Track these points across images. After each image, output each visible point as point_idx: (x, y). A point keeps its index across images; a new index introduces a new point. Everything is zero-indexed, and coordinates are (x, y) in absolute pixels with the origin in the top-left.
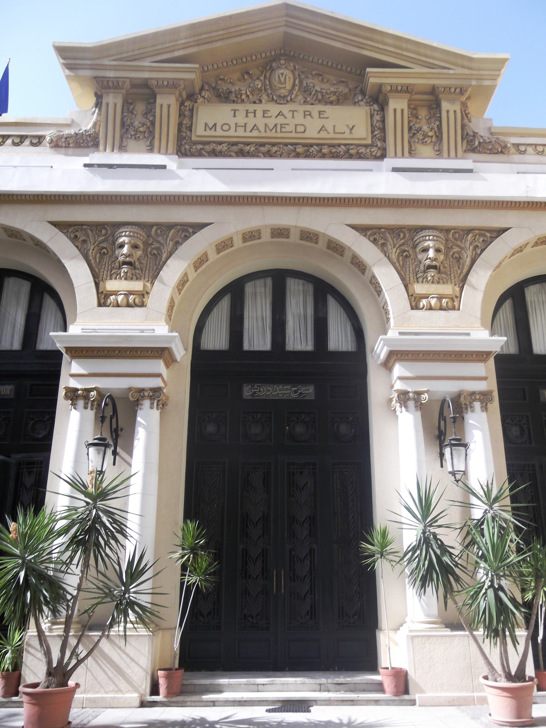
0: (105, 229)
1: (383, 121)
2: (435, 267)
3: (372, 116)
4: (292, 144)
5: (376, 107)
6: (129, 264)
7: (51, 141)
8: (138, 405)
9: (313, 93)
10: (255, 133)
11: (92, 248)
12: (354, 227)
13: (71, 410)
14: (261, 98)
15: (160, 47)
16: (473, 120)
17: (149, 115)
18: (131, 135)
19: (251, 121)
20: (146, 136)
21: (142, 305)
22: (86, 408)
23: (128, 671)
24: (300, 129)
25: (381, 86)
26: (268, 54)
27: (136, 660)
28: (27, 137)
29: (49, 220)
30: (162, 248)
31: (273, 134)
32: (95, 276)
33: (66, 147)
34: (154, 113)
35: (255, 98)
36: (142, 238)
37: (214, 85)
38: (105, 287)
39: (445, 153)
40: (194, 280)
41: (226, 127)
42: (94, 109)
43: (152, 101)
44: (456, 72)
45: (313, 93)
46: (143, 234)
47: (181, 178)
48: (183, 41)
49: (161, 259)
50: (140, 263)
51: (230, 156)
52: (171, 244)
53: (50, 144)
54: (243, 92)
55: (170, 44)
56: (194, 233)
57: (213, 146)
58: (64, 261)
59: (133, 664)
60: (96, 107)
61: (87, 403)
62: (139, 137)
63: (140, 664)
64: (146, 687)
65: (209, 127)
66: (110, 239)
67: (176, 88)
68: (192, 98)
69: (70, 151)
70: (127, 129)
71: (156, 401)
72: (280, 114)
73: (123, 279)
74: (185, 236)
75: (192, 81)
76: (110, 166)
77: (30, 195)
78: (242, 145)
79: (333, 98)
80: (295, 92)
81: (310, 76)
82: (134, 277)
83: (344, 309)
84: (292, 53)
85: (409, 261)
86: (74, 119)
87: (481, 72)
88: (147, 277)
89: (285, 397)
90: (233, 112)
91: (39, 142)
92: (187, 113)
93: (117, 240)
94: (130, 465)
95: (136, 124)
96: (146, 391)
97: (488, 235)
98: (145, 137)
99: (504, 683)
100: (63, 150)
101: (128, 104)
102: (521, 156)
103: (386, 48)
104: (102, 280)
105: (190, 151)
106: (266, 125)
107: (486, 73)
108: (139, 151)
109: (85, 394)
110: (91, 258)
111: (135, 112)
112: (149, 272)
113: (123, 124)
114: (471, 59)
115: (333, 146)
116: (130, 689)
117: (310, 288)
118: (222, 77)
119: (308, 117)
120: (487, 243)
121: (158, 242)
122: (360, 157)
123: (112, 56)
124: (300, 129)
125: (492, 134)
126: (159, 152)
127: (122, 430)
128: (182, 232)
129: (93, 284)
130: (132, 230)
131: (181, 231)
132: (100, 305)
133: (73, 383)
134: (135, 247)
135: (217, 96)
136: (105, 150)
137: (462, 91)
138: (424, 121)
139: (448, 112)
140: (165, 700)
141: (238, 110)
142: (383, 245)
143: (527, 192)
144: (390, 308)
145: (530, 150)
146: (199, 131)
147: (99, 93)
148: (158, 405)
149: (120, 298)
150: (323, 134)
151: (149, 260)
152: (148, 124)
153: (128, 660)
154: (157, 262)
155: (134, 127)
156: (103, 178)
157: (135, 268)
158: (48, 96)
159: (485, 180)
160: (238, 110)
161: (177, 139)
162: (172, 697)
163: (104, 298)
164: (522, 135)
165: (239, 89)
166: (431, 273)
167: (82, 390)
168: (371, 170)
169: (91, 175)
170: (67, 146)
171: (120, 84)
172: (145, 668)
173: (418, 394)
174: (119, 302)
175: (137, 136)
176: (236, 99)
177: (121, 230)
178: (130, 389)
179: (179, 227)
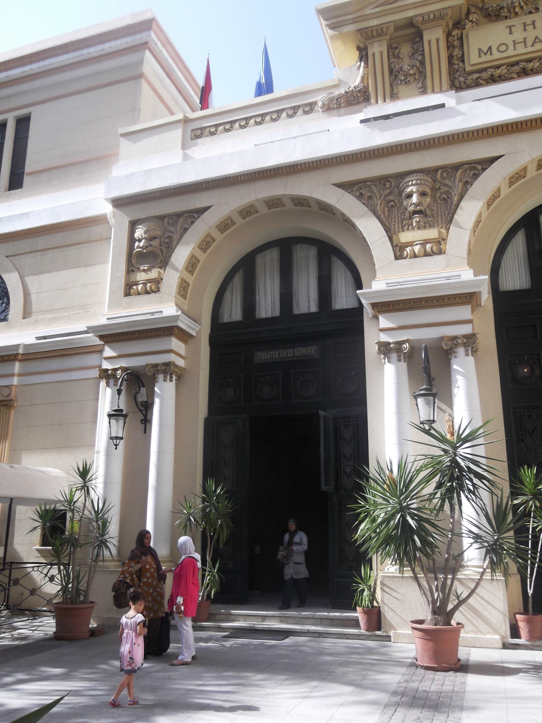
0: (389, 181)
6: (420, 212)
7: (324, 105)
8: (451, 353)
11: (379, 202)
13: (385, 363)
14: (537, 6)
17: (416, 55)
18: (401, 80)
20: (416, 78)
21: (441, 252)
22: (399, 360)
23: (485, 613)
27: (491, 603)
29: (334, 183)
30: (451, 190)
32: (387, 230)
33: (337, 108)
34: (422, 52)
35: (530, 8)
36: (429, 184)
37: (481, 5)
38: (399, 239)
40: (486, 220)
41: (503, 48)
42: (359, 63)
43: (417, 40)
46: (430, 180)
47: (464, 114)
49: (452, 203)
50: (431, 210)
52: (460, 185)
53: (322, 108)
54: (516, 4)
56: (484, 170)
57: (490, 72)
58: (354, 220)
59: (489, 607)
60: (361, 61)
61: (400, 356)
62: (409, 81)
63: (496, 607)
64: (506, 629)
65: (483, 52)
66: (396, 191)
67: (444, 19)
68: (459, 26)
69: (342, 111)
70: (396, 76)
71: (470, 348)
73: (416, 228)
74: (474, 174)
76: (387, 117)
77: (313, 162)
78: (524, 63)
82: (427, 225)
88: (440, 223)
90: (508, 29)
91: (311, 109)
92: (456, 43)
93: (403, 191)
95: (406, 67)
96: (460, 338)
98: (415, 79)
100: (335, 112)
101: (393, 50)
104: (395, 233)
105: (465, 83)
108: (412, 96)
109: (397, 347)
110: (380, 213)
111: (401, 56)
112: (441, 218)
113: (391, 71)
116: (490, 630)
121: (446, 185)
123: (373, 3)
126: (433, 92)
127: (434, 379)
128: (470, 170)
129: (387, 238)
130: (418, 178)
131: (468, 170)
132: (397, 258)
133: (384, 338)
134: (423, 194)
135: (485, 17)
136: (377, 102)
140: (528, 643)
141: (514, 26)
146: (474, 58)
147: (362, 45)
148: (472, 351)
149: (417, 249)
151: (439, 205)
152: (418, 64)
153: (483, 602)
154: (449, 206)
155: (404, 71)
157: (426, 216)
160: (514, 26)
161: (449, 74)
162: (535, 641)
163: (399, 251)
165: (512, 2)
167: (394, 343)
169: (368, 130)
171: (384, 30)
172: (502, 611)
174: (416, 252)
175: (407, 80)
176: (508, 14)
177: (406, 180)
178: (442, 338)
179: (466, 166)
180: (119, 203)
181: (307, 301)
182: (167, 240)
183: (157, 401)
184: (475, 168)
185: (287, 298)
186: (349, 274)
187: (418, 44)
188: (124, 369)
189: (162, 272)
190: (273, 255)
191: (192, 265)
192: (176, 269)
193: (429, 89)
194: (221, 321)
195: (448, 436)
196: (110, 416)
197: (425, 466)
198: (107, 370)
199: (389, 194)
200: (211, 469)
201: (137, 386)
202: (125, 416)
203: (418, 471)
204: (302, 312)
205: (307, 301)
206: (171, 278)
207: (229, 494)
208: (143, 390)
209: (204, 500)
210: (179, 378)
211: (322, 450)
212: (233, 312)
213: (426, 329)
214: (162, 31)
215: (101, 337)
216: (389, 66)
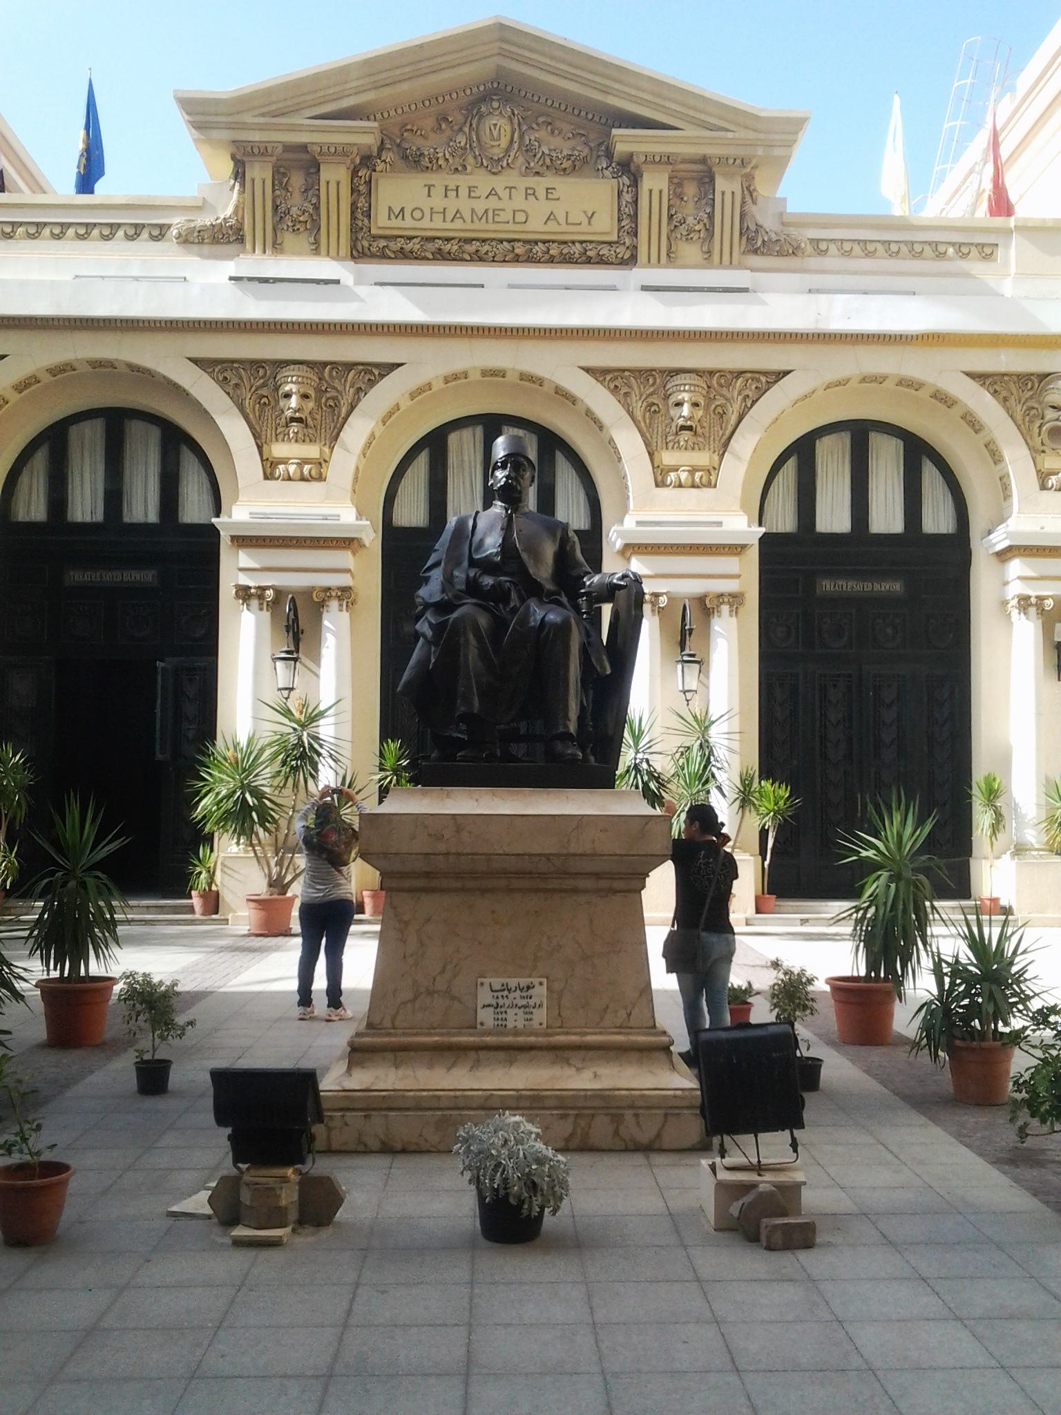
1: (636, 202)
2: (690, 428)
3: (620, 193)
4: (509, 241)
6: (300, 420)
7: (179, 236)
9: (538, 156)
10: (458, 224)
12: (587, 370)
15: (322, 93)
16: (760, 201)
17: (311, 193)
19: (452, 204)
21: (321, 478)
22: (261, 609)
24: (520, 217)
25: (632, 155)
26: (475, 90)
28: (143, 226)
31: (482, 225)
32: (256, 436)
35: (455, 162)
39: (716, 258)
41: (417, 214)
43: (312, 170)
44: (737, 135)
45: (538, 156)
48: (355, 84)
50: (314, 419)
55: (338, 89)
56: (382, 376)
57: (400, 243)
69: (206, 249)
72: (493, 192)
76: (265, 280)
79: (566, 164)
80: (512, 154)
81: (534, 126)
83: (577, 472)
84: (509, 89)
85: (659, 419)
86: (208, 199)
94: (317, 676)
95: (294, 211)
97: (763, 379)
100: (195, 247)
101: (280, 176)
102: (820, 259)
106: (473, 210)
107: (777, 137)
113: (276, 208)
114: (757, 118)
115: (565, 243)
118: (409, 127)
119: (531, 198)
120: (761, 392)
122: (602, 262)
124: (520, 217)
125: (783, 224)
126: (328, 254)
132: (266, 478)
133: (244, 580)
134: (305, 396)
137: (743, 164)
138: (691, 205)
139: (723, 193)
143: (817, 321)
144: (629, 483)
145: (833, 248)
146: (381, 221)
147: (238, 157)
149: (292, 469)
150: (552, 227)
158: (170, 167)
159: (764, 303)
164: (825, 226)
166: (686, 435)
170: (202, 242)
171: (270, 150)
184: (371, 373)
185: (114, 497)
187: (314, 176)
195: (297, 714)
197: (270, 744)
199: (264, 385)
203: (262, 750)
204: (135, 521)
205: (143, 506)
211: (158, 711)
213: (298, 573)
216: (274, 201)
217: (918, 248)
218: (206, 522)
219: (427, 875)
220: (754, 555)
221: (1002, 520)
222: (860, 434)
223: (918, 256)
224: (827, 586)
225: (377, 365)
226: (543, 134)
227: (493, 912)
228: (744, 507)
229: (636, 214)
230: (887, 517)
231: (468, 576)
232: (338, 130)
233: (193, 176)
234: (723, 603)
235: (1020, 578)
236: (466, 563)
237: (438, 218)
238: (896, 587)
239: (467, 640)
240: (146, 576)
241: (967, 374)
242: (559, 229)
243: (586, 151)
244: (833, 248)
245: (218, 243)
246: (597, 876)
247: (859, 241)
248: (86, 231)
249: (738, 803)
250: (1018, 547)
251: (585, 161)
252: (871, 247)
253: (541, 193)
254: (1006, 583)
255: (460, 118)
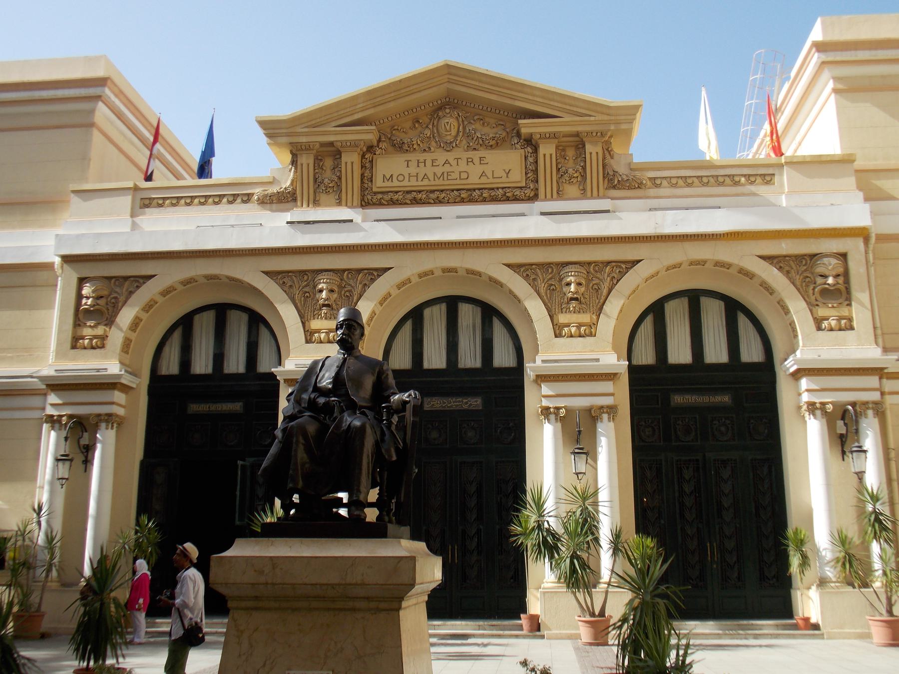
1: (536, 162)
2: (576, 299)
3: (526, 158)
4: (458, 190)
5: (529, 149)
6: (328, 306)
7: (259, 199)
10: (426, 182)
12: (508, 266)
16: (615, 157)
19: (422, 171)
24: (464, 176)
25: (531, 134)
31: (441, 182)
32: (301, 316)
41: (401, 178)
47: (365, 231)
48: (361, 105)
51: (406, 204)
56: (379, 276)
57: (390, 195)
69: (274, 206)
72: (447, 162)
75: (371, 140)
80: (459, 139)
84: (456, 101)
87: (618, 118)
89: (458, 408)
92: (368, 165)
97: (624, 266)
99: (588, 618)
101: (318, 159)
103: (535, 99)
107: (623, 117)
113: (315, 180)
115: (493, 189)
117: (479, 309)
120: (623, 274)
122: (516, 199)
124: (464, 176)
125: (631, 169)
129: (301, 324)
132: (308, 342)
134: (332, 291)
138: (571, 161)
139: (591, 153)
142: (534, 279)
145: (665, 183)
146: (379, 183)
149: (322, 336)
150: (484, 180)
156: (303, 233)
159: (620, 219)
164: (659, 169)
166: (574, 304)
168: (523, 215)
170: (272, 203)
173: (558, 409)
180: (68, 259)
181: (235, 363)
182: (113, 301)
183: (99, 446)
185: (219, 359)
186: (273, 342)
188: (71, 417)
189: (108, 329)
190: (210, 316)
191: (135, 324)
192: (121, 330)
193: (344, 202)
194: (159, 373)
196: (58, 460)
198: (52, 416)
199: (306, 286)
200: (144, 506)
201: (80, 434)
202: (71, 460)
205: (235, 363)
206: (116, 337)
207: (159, 526)
208: (86, 435)
209: (136, 532)
210: (119, 424)
211: (238, 493)
212: (171, 366)
214: (115, 85)
215: (48, 385)
216: (314, 176)
217: (721, 179)
218: (268, 371)
219: (256, 598)
220: (625, 379)
221: (794, 351)
222: (694, 299)
223: (722, 184)
224: (678, 399)
225: (376, 270)
226: (478, 126)
227: (299, 625)
228: (616, 348)
229: (537, 169)
230: (716, 352)
231: (310, 398)
232: (352, 133)
233: (269, 165)
234: (603, 412)
235: (807, 390)
236: (311, 389)
237: (413, 179)
238: (725, 399)
239: (297, 441)
240: (236, 407)
241: (761, 257)
242: (489, 181)
243: (504, 134)
244: (665, 183)
245: (281, 202)
246: (367, 598)
247: (681, 177)
248: (205, 200)
249: (611, 551)
250: (805, 370)
251: (504, 140)
252: (689, 181)
253: (477, 161)
254: (800, 395)
255: (427, 120)
